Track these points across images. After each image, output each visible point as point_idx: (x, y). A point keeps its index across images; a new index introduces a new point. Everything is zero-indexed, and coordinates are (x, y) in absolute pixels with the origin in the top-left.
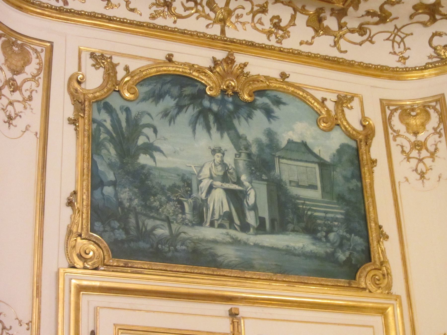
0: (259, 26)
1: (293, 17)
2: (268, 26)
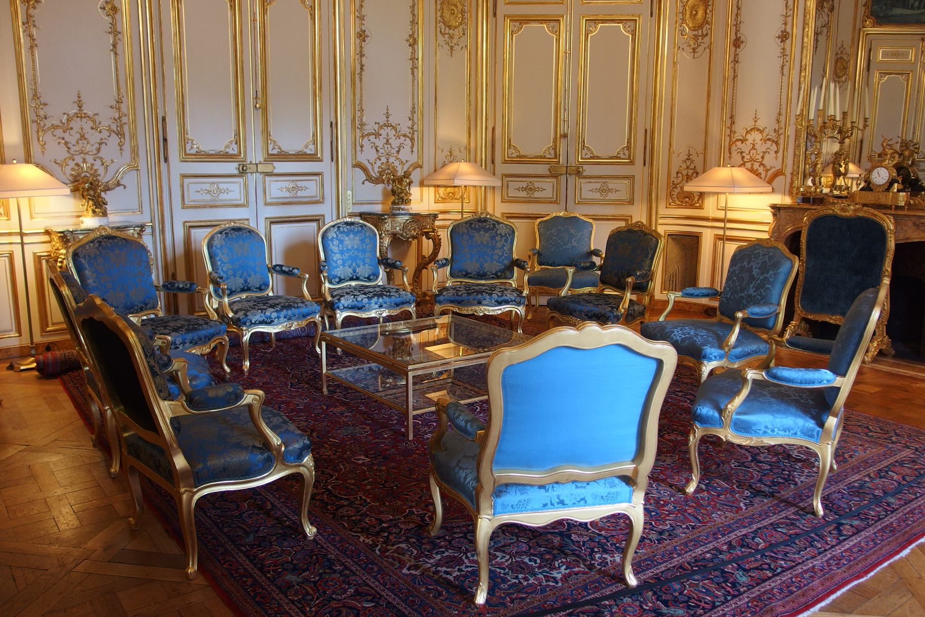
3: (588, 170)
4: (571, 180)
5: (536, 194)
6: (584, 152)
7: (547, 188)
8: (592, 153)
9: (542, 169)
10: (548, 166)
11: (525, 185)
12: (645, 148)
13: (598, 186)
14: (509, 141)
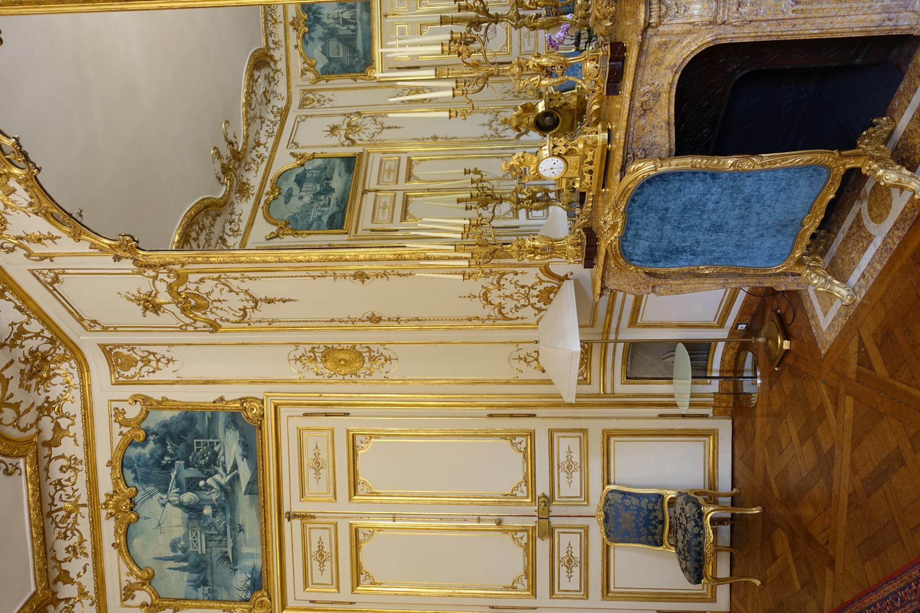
0: (72, 480)
1: (57, 458)
2: (70, 473)
3: (543, 488)
4: (555, 510)
5: (576, 554)
6: (519, 494)
7: (568, 542)
8: (520, 484)
9: (543, 546)
10: (538, 540)
11: (564, 570)
12: (511, 416)
13: (563, 475)
14: (507, 588)
